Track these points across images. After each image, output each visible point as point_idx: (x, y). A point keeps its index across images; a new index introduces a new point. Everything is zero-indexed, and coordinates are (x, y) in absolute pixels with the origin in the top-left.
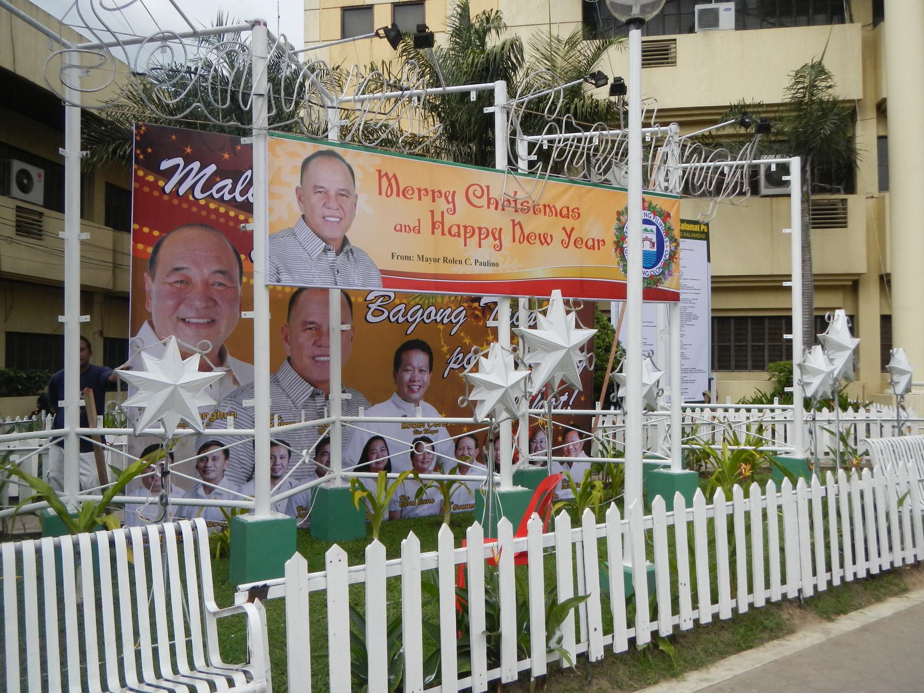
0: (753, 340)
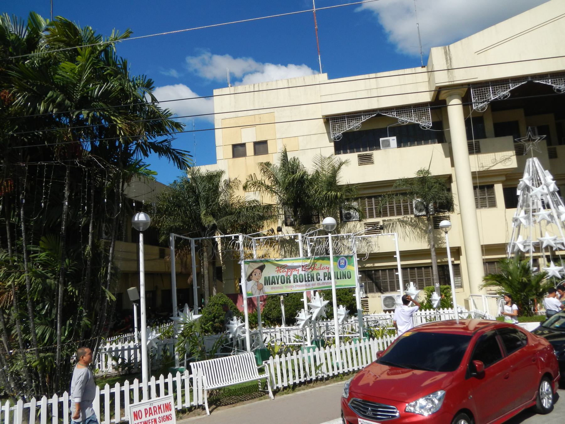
0: (418, 277)
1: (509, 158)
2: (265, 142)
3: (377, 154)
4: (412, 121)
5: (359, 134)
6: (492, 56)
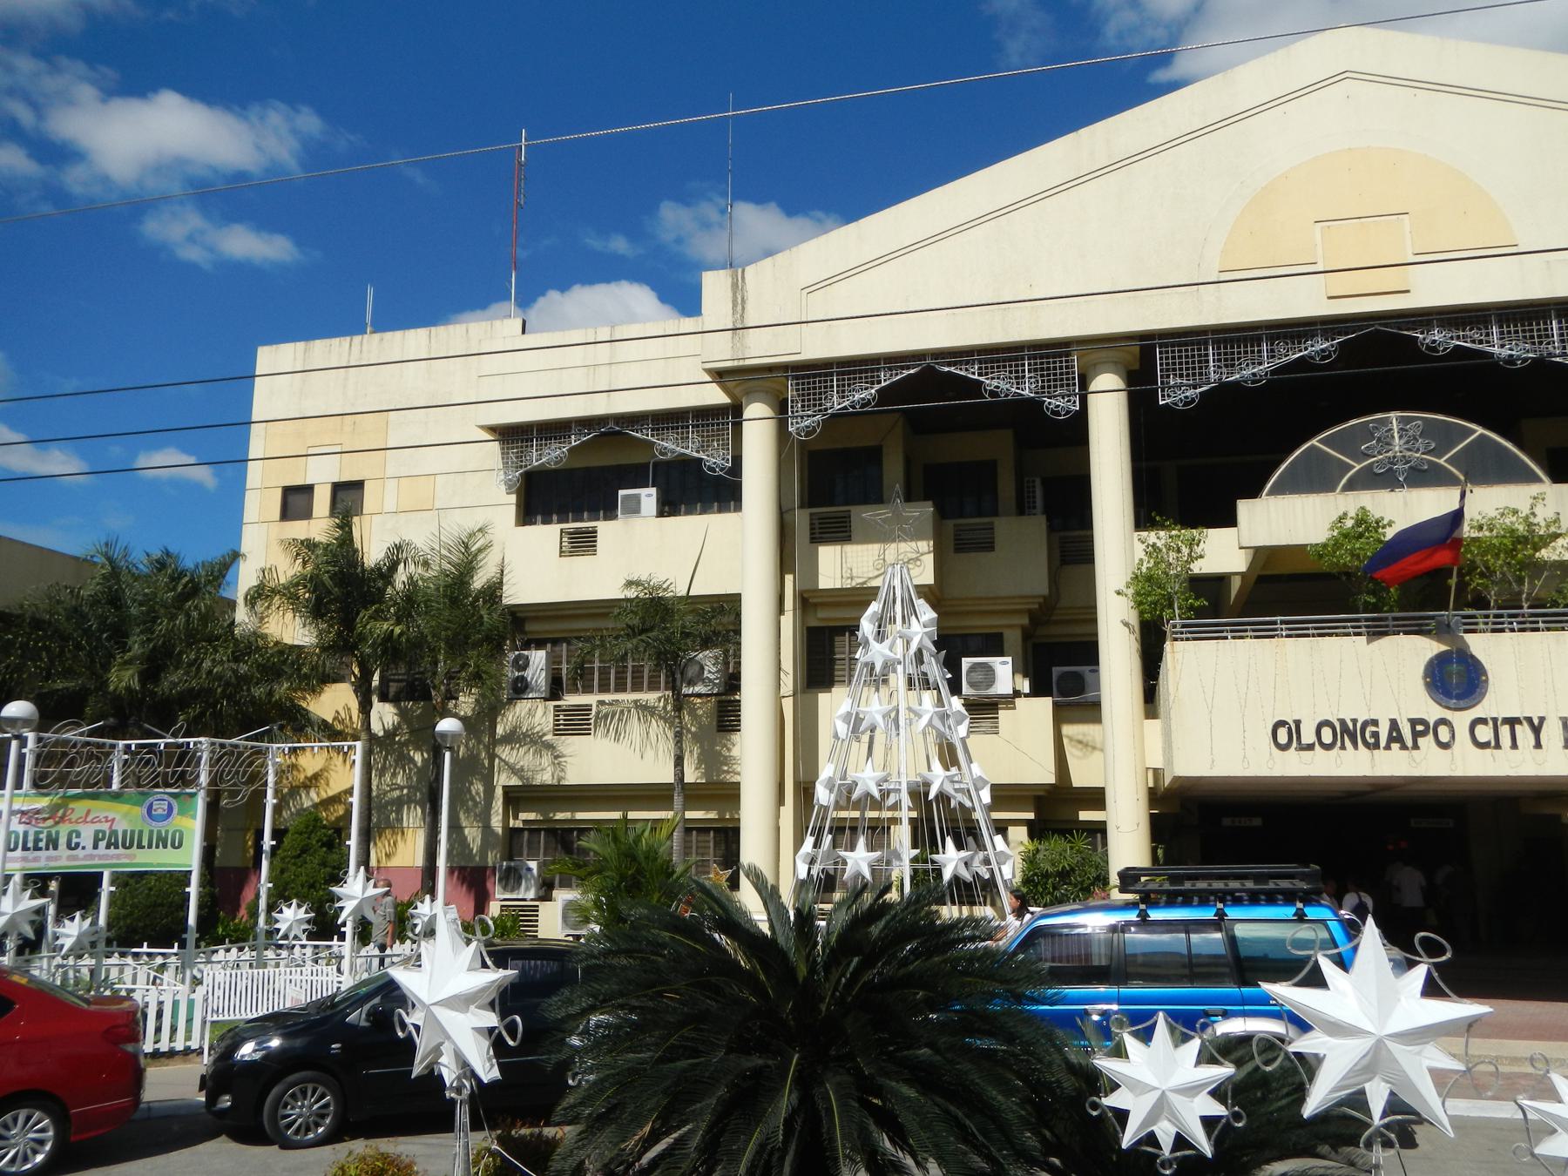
1: (917, 559)
2: (358, 485)
3: (604, 528)
4: (688, 452)
5: (573, 474)
6: (842, 299)
